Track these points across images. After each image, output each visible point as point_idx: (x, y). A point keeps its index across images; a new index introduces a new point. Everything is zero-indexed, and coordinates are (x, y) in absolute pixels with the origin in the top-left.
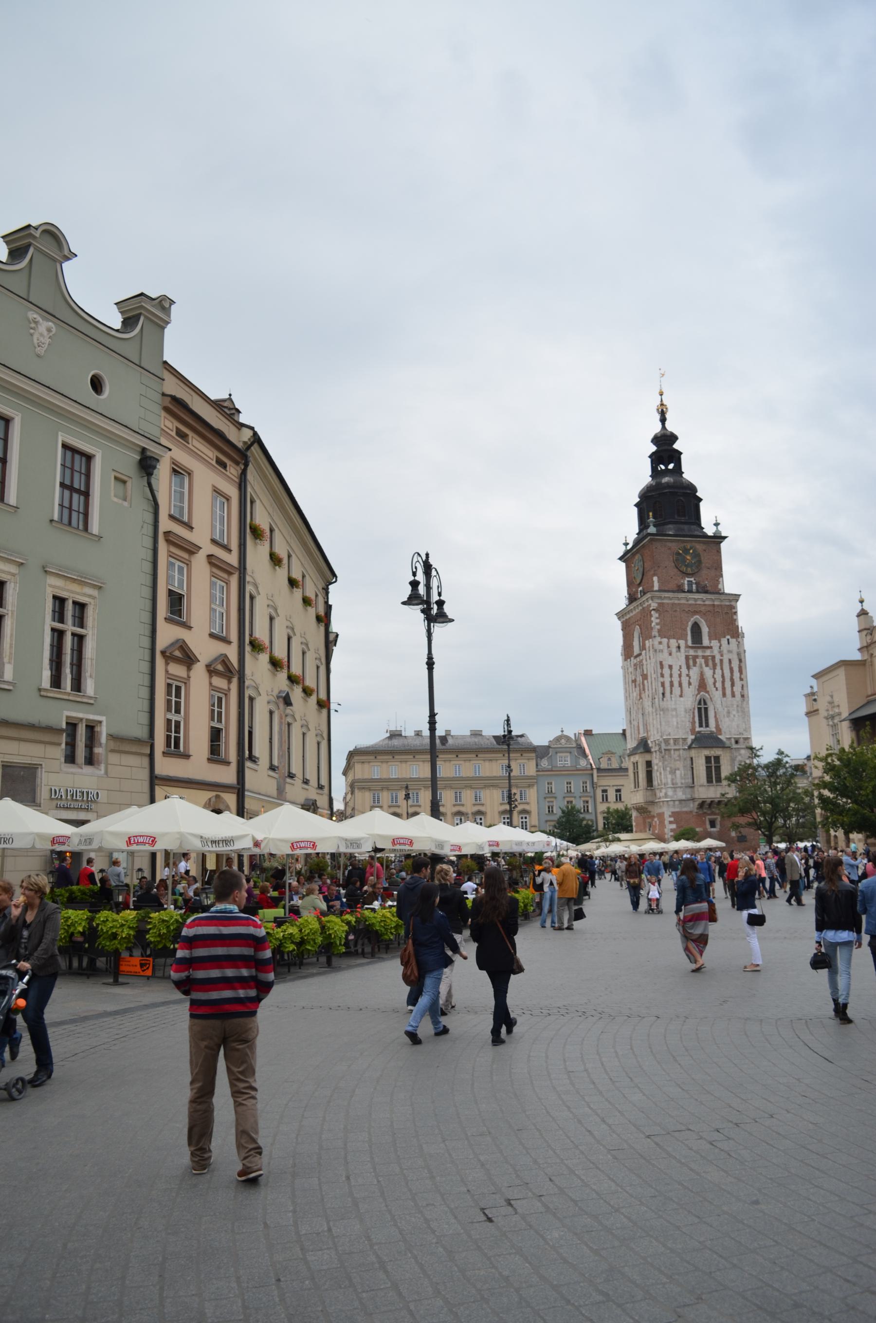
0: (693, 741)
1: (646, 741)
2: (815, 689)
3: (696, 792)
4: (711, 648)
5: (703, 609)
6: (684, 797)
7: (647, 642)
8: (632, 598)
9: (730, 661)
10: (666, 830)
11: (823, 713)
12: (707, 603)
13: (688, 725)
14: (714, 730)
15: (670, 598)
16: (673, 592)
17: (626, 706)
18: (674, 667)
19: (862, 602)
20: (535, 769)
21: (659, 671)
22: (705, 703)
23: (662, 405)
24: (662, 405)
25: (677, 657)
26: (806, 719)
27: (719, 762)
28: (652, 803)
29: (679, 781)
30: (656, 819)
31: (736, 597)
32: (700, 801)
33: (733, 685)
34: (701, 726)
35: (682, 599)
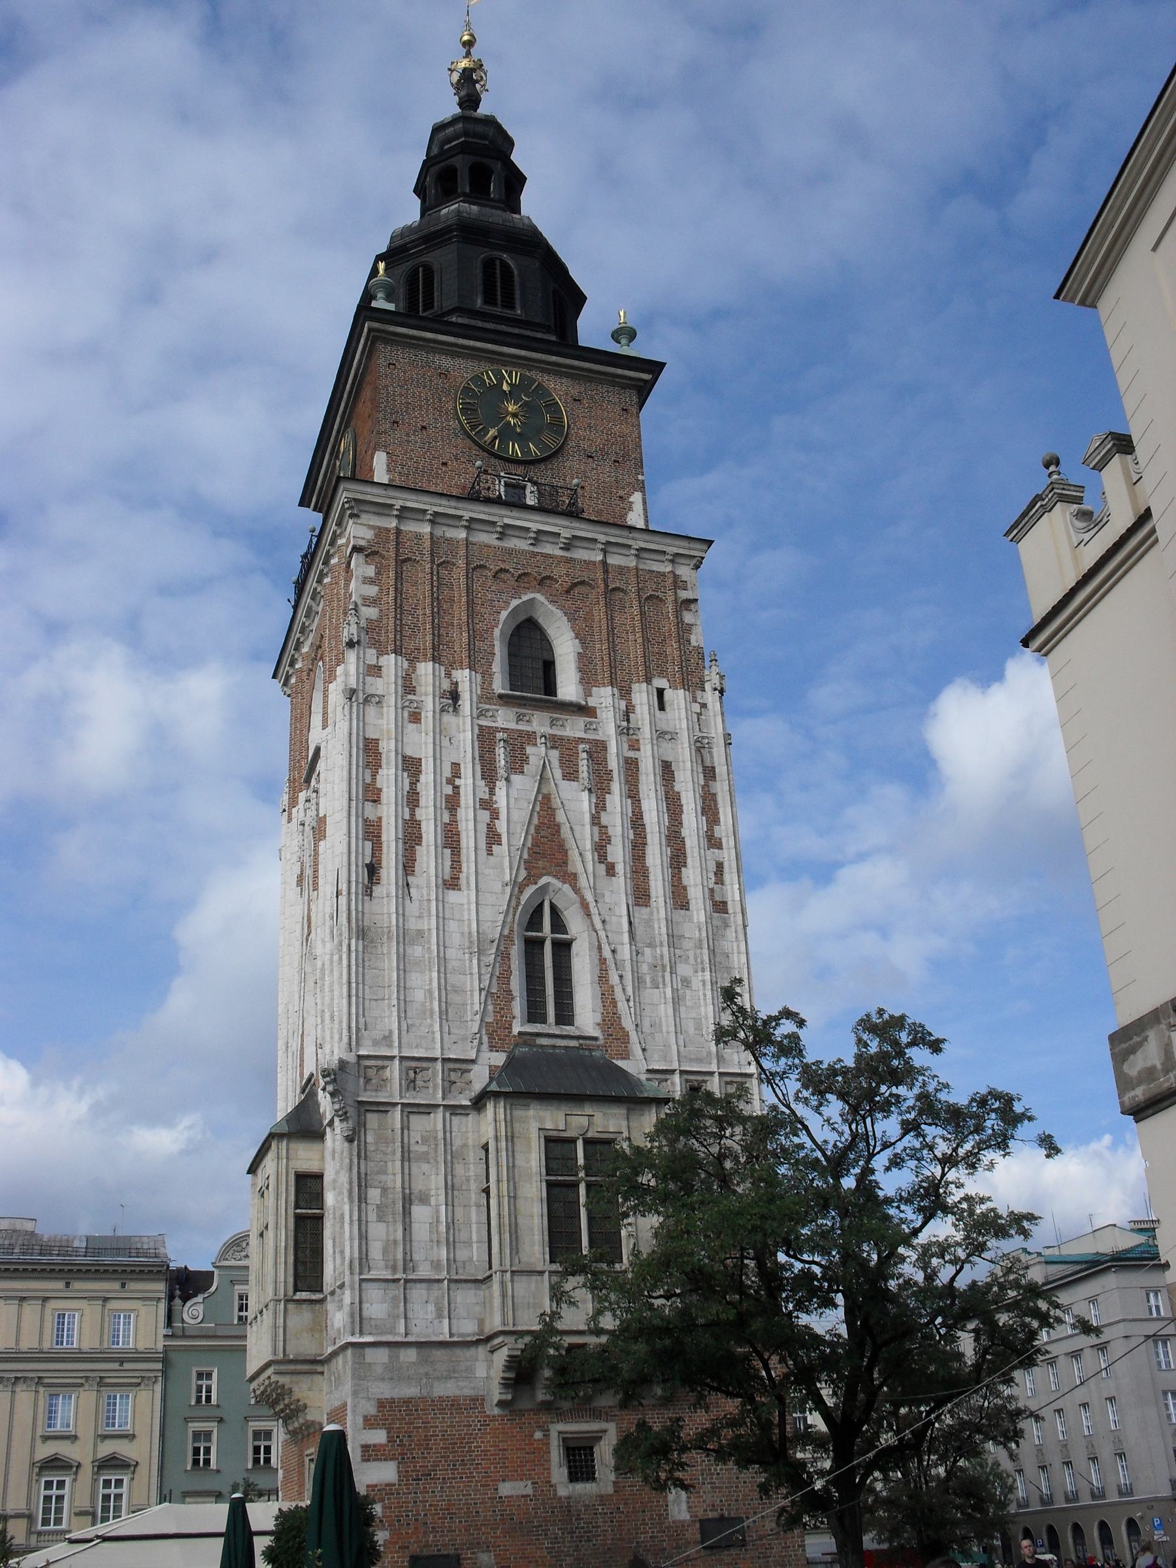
5: (558, 571)
13: (475, 1001)
14: (596, 1032)
18: (428, 767)
20: (163, 1331)
22: (558, 924)
33: (678, 860)
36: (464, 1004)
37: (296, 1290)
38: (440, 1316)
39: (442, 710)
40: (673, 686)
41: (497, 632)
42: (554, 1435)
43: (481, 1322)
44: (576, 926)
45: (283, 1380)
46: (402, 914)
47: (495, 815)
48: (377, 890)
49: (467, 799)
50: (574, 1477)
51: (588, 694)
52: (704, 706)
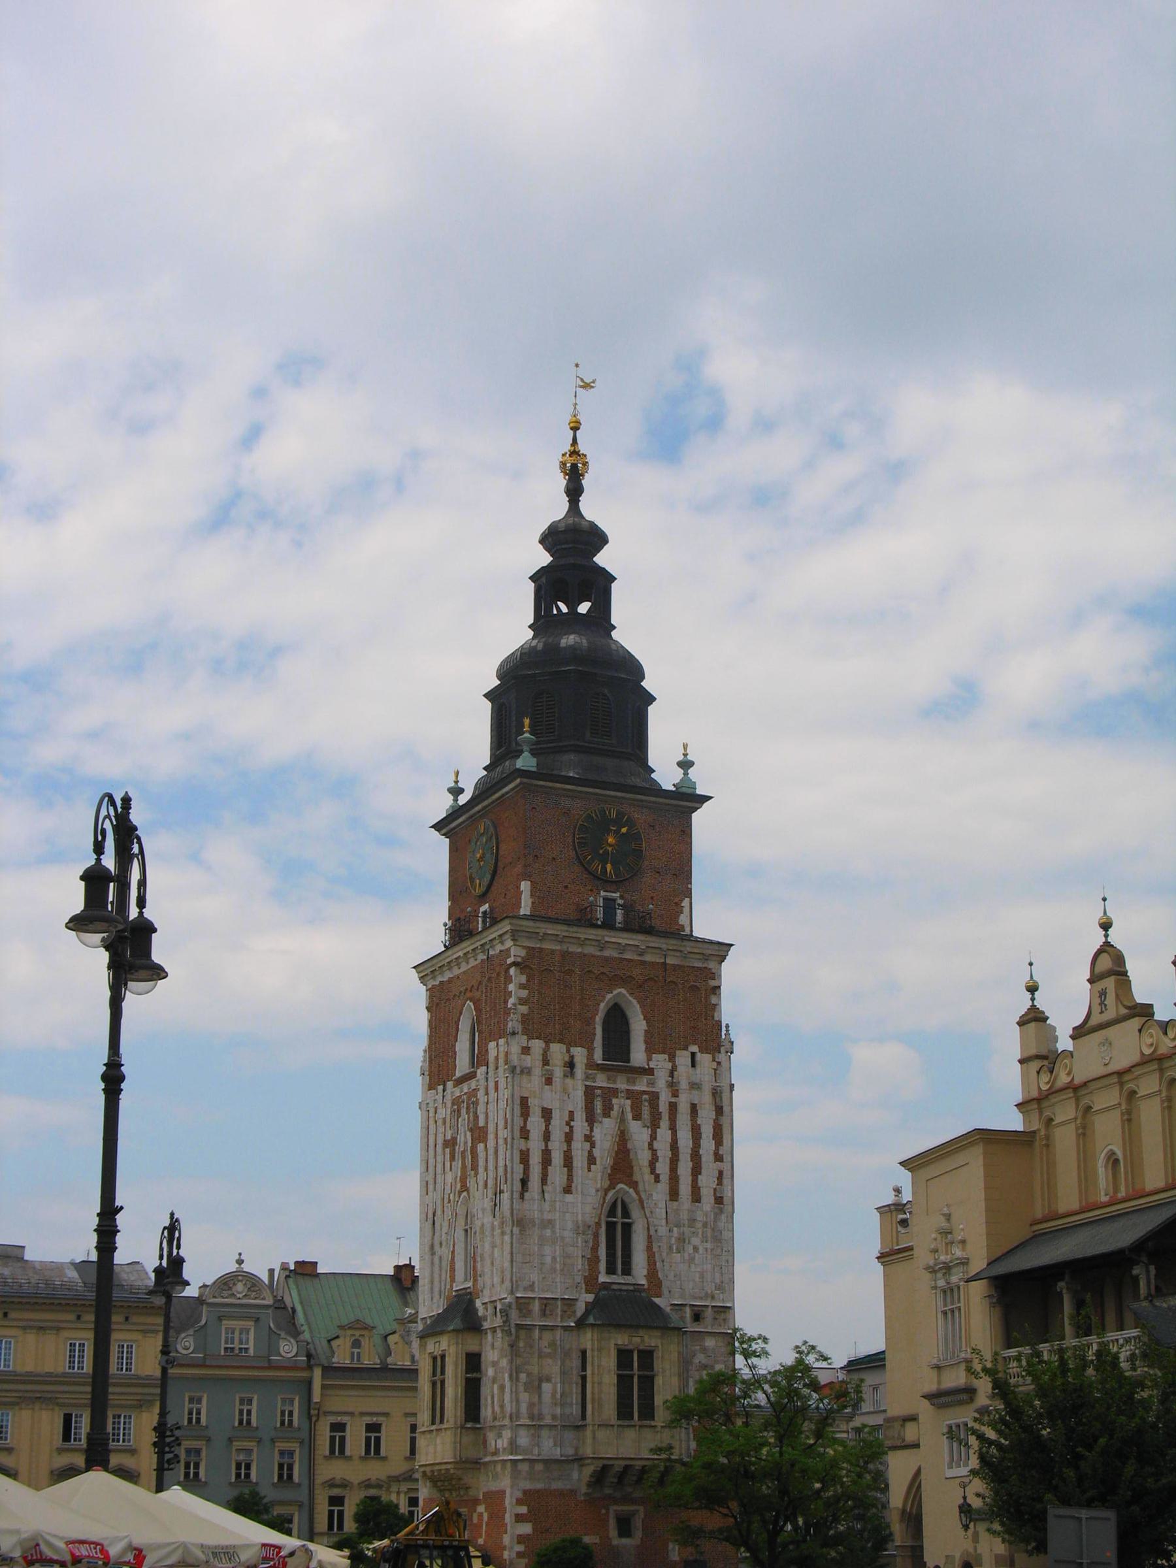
0: (590, 1308)
1: (471, 1302)
2: (907, 1196)
3: (589, 1441)
4: (650, 1072)
5: (636, 972)
6: (557, 1453)
7: (492, 1045)
8: (459, 930)
9: (694, 1109)
10: (506, 1539)
11: (923, 1257)
12: (648, 958)
13: (579, 1264)
14: (643, 1282)
15: (556, 939)
16: (568, 923)
17: (422, 1203)
18: (556, 1115)
19: (1032, 989)
21: (519, 1122)
22: (626, 1213)
23: (574, 453)
24: (574, 453)
25: (565, 1090)
26: (880, 1268)
27: (651, 1367)
28: (475, 1464)
29: (546, 1411)
30: (481, 1508)
31: (721, 950)
32: (600, 1463)
33: (696, 1170)
34: (611, 1270)
35: (589, 943)
36: (573, 1265)
37: (466, 1421)
38: (555, 1445)
39: (565, 1076)
40: (701, 1051)
42: (611, 1511)
43: (577, 1449)
44: (635, 1213)
45: (459, 1472)
46: (541, 1211)
47: (593, 1145)
48: (527, 1195)
49: (578, 1135)
50: (621, 1535)
51: (649, 1059)
52: (719, 1063)
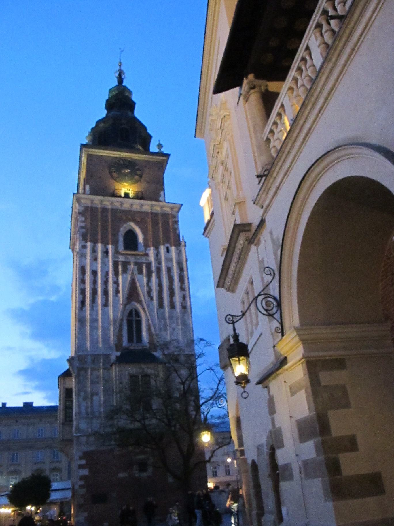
4: (146, 255)
14: (148, 345)
22: (138, 314)
41: (120, 234)
47: (118, 285)
48: (84, 308)
